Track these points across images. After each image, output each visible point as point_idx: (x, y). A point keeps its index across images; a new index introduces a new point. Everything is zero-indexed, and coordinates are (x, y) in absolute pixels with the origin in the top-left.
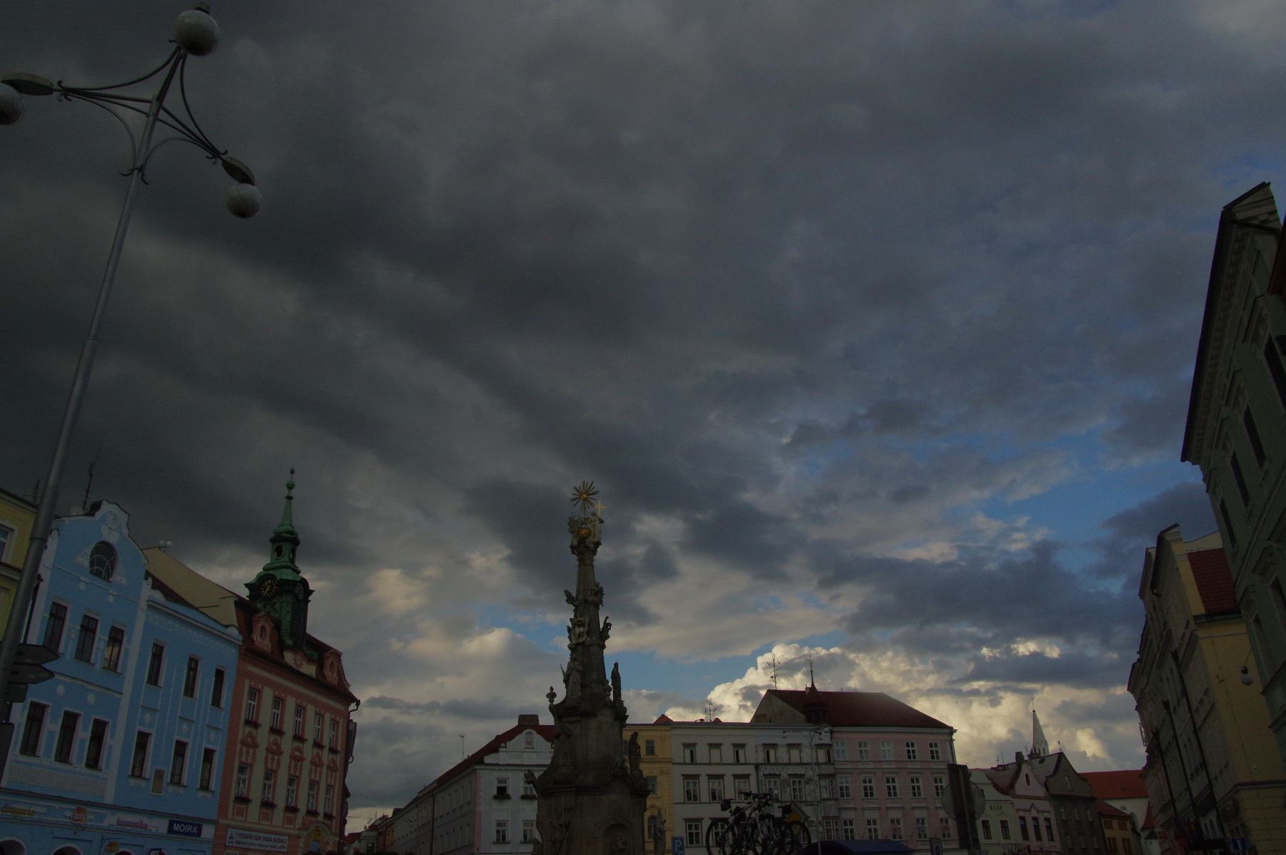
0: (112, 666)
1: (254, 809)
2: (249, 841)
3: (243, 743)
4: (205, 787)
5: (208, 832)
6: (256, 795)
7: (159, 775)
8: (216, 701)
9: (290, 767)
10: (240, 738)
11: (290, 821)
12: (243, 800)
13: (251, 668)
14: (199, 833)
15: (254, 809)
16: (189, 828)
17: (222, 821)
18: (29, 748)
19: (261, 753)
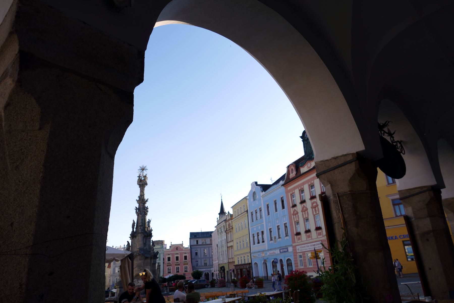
0: (261, 217)
1: (303, 236)
2: (305, 248)
3: (293, 215)
4: (287, 235)
5: (290, 249)
6: (302, 231)
7: (275, 238)
8: (283, 207)
9: (313, 212)
10: (292, 212)
11: (320, 234)
12: (298, 234)
13: (289, 188)
14: (288, 251)
15: (303, 236)
16: (285, 250)
17: (294, 244)
18: (254, 244)
19: (300, 214)
